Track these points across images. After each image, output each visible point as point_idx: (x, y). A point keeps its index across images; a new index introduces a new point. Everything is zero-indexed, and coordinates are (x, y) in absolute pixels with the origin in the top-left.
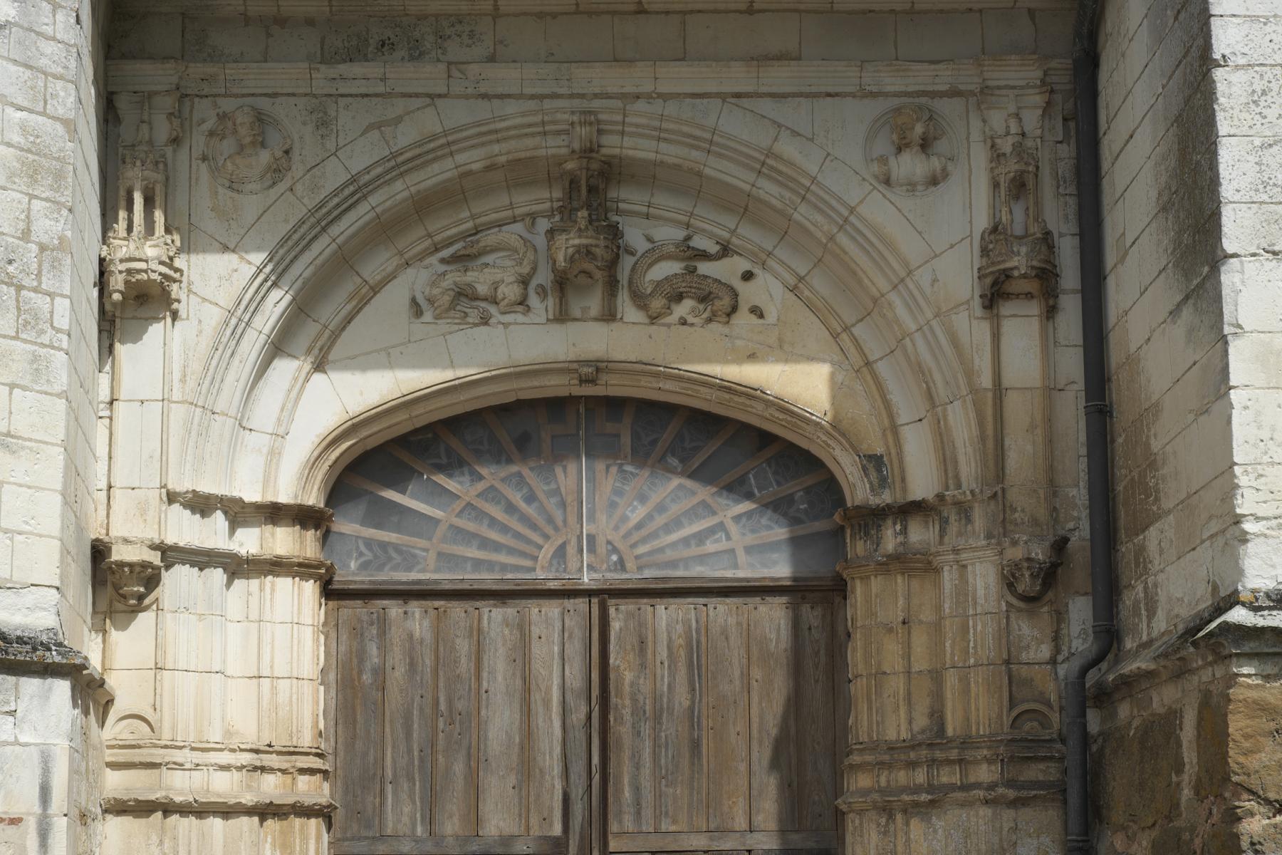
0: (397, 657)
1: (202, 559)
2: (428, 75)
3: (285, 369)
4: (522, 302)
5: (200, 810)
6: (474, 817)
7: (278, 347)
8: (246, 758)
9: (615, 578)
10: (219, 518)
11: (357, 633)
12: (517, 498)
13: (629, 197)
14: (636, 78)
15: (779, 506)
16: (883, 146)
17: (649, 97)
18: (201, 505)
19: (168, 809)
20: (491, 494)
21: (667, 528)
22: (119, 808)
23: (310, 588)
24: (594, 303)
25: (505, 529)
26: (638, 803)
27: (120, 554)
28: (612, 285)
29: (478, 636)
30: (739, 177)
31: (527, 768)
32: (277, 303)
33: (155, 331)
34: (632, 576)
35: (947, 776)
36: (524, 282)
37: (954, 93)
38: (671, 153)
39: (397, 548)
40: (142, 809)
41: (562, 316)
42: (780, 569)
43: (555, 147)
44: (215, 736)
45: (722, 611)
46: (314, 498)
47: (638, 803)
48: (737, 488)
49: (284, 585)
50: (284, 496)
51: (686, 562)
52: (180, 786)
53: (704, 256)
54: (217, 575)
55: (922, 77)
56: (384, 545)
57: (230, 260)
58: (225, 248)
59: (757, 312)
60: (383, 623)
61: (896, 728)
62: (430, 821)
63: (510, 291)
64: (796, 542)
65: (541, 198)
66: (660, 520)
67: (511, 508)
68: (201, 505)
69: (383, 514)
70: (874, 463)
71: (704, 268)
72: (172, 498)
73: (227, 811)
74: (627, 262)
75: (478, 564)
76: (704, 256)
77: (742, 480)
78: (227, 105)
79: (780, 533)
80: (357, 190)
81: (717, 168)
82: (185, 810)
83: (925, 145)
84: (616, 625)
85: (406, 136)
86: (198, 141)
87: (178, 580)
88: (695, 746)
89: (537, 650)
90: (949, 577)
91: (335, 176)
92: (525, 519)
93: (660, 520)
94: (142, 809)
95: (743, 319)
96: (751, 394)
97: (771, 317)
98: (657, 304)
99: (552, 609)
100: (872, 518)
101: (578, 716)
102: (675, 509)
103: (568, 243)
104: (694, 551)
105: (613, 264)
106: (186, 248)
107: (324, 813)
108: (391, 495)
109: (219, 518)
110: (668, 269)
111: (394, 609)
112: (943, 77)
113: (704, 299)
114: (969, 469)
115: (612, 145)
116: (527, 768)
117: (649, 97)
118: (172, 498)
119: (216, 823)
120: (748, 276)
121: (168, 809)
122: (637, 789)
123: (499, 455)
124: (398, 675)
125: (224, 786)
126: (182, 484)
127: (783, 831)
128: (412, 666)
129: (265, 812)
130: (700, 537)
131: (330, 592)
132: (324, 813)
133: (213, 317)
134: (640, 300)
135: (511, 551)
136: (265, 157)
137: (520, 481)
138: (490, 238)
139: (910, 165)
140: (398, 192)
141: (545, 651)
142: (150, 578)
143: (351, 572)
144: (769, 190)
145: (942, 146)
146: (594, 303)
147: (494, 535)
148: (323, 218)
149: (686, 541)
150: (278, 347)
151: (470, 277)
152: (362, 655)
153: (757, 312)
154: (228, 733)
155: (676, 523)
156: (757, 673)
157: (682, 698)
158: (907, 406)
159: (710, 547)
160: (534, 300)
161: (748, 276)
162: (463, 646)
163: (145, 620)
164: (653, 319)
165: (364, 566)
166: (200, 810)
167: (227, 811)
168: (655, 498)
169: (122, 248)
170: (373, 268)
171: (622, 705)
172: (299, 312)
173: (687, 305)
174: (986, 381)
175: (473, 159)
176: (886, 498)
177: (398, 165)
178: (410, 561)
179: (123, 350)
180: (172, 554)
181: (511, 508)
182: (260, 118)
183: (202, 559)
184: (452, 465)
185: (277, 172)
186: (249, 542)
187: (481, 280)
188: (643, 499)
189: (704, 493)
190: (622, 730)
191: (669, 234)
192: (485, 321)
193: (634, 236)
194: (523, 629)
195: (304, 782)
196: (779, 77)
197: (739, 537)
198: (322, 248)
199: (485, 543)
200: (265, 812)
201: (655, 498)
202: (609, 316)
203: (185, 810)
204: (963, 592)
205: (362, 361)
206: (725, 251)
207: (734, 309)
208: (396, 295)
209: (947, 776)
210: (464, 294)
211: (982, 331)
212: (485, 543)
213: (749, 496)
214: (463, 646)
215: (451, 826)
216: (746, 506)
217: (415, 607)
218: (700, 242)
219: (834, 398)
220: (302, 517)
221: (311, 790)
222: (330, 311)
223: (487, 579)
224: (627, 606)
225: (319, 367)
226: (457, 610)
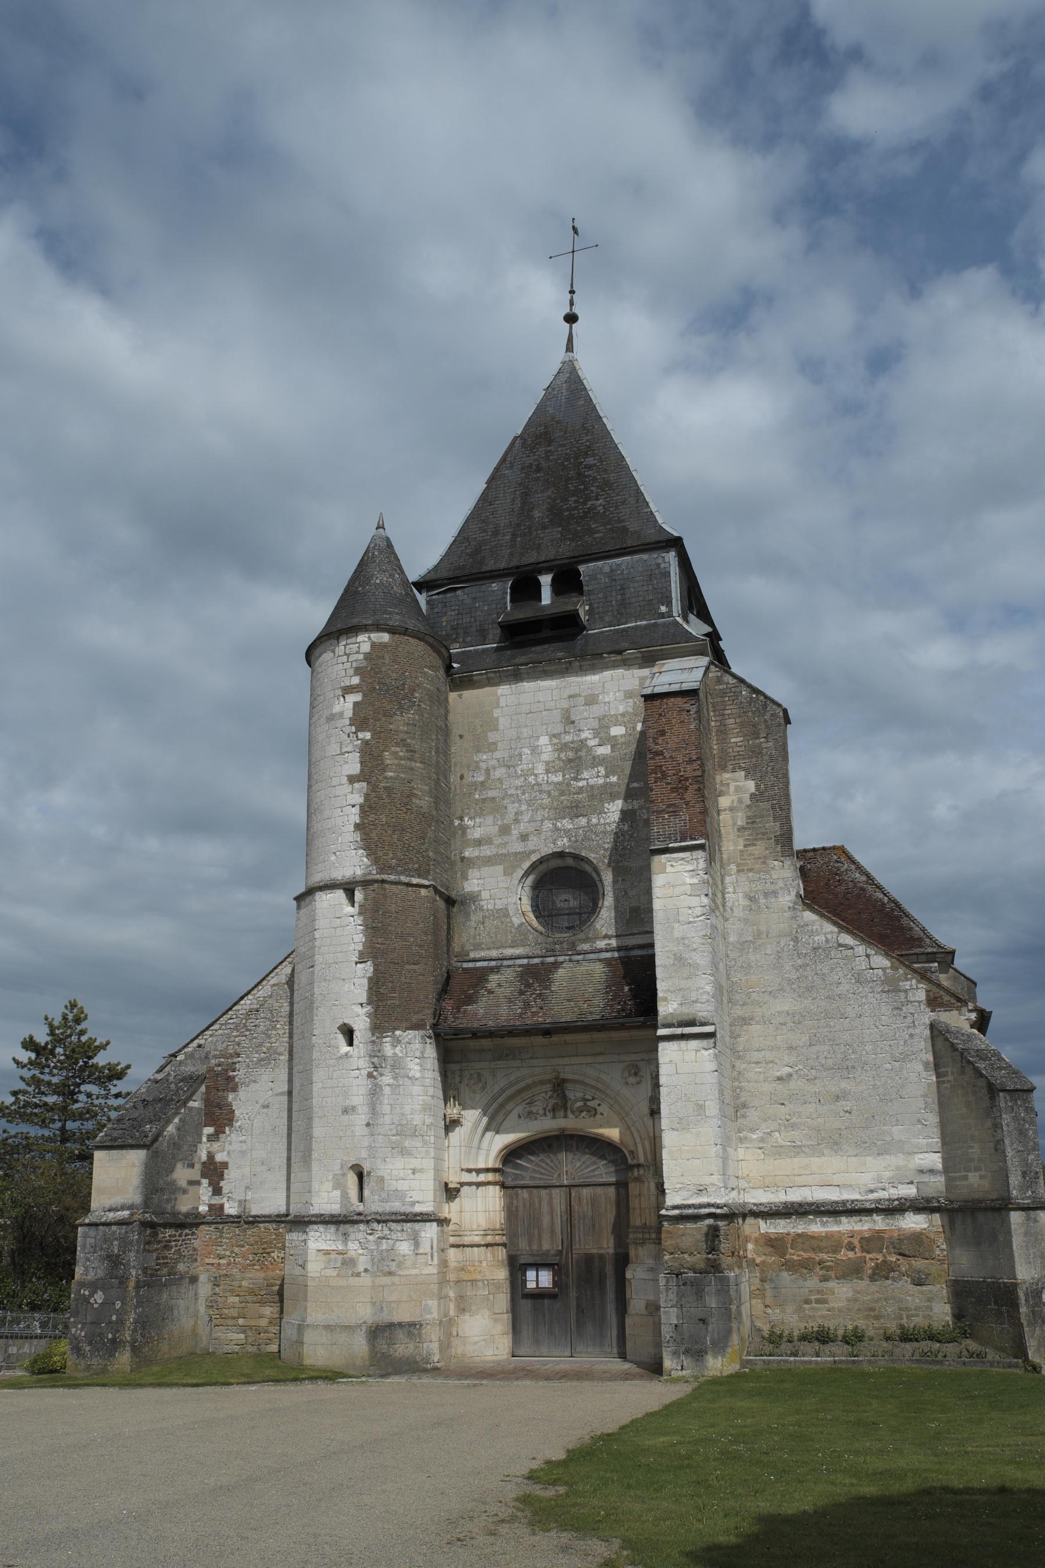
0: (521, 1204)
1: (470, 1184)
2: (518, 1063)
3: (489, 1134)
4: (545, 1114)
5: (472, 1246)
6: (540, 1245)
7: (487, 1129)
8: (482, 1233)
9: (573, 1182)
10: (474, 1173)
11: (511, 1197)
12: (548, 1161)
13: (569, 1086)
14: (566, 1061)
15: (613, 1162)
16: (626, 1074)
17: (569, 1065)
18: (469, 1171)
19: (464, 1246)
20: (542, 1160)
21: (586, 1168)
22: (453, 1246)
23: (497, 1187)
24: (562, 1113)
25: (546, 1169)
26: (580, 1241)
27: (451, 1186)
28: (566, 1109)
29: (540, 1197)
30: (593, 1083)
31: (552, 1232)
32: (485, 1120)
33: (457, 1129)
34: (577, 1181)
35: (647, 1236)
36: (545, 1109)
37: (643, 1060)
38: (576, 1077)
39: (521, 1175)
40: (458, 1246)
41: (554, 1117)
42: (613, 1179)
43: (548, 1077)
44: (475, 1227)
45: (599, 1190)
46: (498, 1165)
47: (580, 1241)
48: (603, 1157)
49: (491, 1187)
50: (490, 1166)
51: (591, 1177)
52: (467, 1240)
53: (588, 1100)
54: (474, 1187)
55: (634, 1057)
56: (517, 1174)
57: (474, 1111)
58: (473, 1108)
59: (602, 1114)
60: (517, 1195)
61: (638, 1223)
62: (530, 1246)
63: (541, 1112)
64: (616, 1171)
65: (548, 1087)
66: (584, 1166)
67: (547, 1164)
68: (469, 1171)
69: (517, 1166)
70: (632, 1152)
71: (589, 1103)
72: (462, 1170)
73: (478, 1246)
74: (569, 1103)
75: (540, 1179)
76: (588, 1100)
77: (604, 1155)
78: (472, 1072)
79: (613, 1169)
80: (502, 1091)
81: (587, 1080)
82: (468, 1246)
83: (636, 1074)
84: (573, 1194)
85: (513, 1077)
86: (466, 1081)
87: (465, 1190)
88: (594, 1226)
89: (554, 1201)
90: (646, 1184)
91: (497, 1089)
92: (550, 1167)
93: (584, 1166)
94: (458, 1246)
95: (598, 1116)
96: (602, 1135)
97: (605, 1116)
98: (577, 1113)
99: (557, 1190)
100: (631, 1167)
101: (565, 1218)
102: (587, 1163)
103: (553, 1101)
104: (592, 1174)
105: (566, 1103)
106: (463, 1109)
107: (504, 1245)
108: (519, 1161)
109: (474, 1173)
110: (580, 1104)
111: (520, 1191)
112: (639, 1056)
113: (589, 1111)
114: (649, 1157)
115: (562, 1076)
116: (552, 1232)
117: (569, 1065)
118: (462, 1170)
119: (476, 1249)
120: (599, 1105)
121: (464, 1246)
122: (579, 1238)
123: (544, 1151)
124: (521, 1208)
125: (477, 1240)
126: (465, 1166)
127: (615, 1248)
128: (524, 1206)
129: (487, 1245)
130: (594, 1170)
131: (503, 1186)
132: (504, 1245)
133: (470, 1125)
134: (573, 1112)
135: (547, 1175)
136: (480, 1085)
137: (549, 1157)
138: (536, 1098)
139: (632, 1080)
140: (513, 1090)
141: (556, 1201)
142: (458, 1190)
143: (509, 1182)
144: (600, 1086)
145: (641, 1073)
146: (562, 1113)
147: (543, 1171)
148: (494, 1099)
149: (591, 1171)
150: (487, 1129)
151: (532, 1108)
152: (512, 1203)
153: (602, 1114)
154: (478, 1226)
155: (588, 1167)
156: (609, 1206)
157: (590, 1214)
158: (638, 1140)
159: (596, 1173)
160: (548, 1113)
161: (599, 1105)
162: (536, 1200)
163: (457, 1200)
164: (576, 1117)
165: (513, 1180)
166: (472, 1246)
167: (478, 1246)
168: (583, 1160)
169: (449, 1111)
170: (509, 1107)
171: (575, 1215)
172: (491, 1119)
173: (585, 1113)
174: (652, 1135)
175: (529, 1081)
176: (635, 1162)
177: (512, 1084)
178: (523, 1178)
179: (450, 1134)
180: (462, 1184)
181: (547, 1164)
182: (479, 1075)
183: (470, 1184)
184: (532, 1153)
185: (484, 1088)
186: (482, 1177)
187: (534, 1109)
188: (579, 1160)
189: (594, 1159)
190: (576, 1222)
191: (580, 1095)
192: (536, 1119)
193: (571, 1095)
194: (550, 1195)
195: (497, 1237)
196: (600, 1059)
197: (603, 1170)
198: (495, 1105)
199: (541, 1173)
200: (487, 1245)
201: (583, 1160)
202: (566, 1117)
203: (468, 1246)
204: (649, 1189)
205: (507, 1131)
206: (593, 1099)
207: (596, 1114)
208: (515, 1113)
209: (647, 1236)
210: (530, 1113)
211: (651, 1121)
212: (541, 1173)
213: (606, 1159)
214: (536, 1200)
215: (535, 1247)
216: (605, 1162)
217: (525, 1190)
218: (588, 1097)
219: (620, 1136)
220: (494, 1170)
221: (498, 1239)
222: (499, 1118)
223: (541, 1183)
224: (576, 1189)
225: (497, 1132)
226: (535, 1191)
